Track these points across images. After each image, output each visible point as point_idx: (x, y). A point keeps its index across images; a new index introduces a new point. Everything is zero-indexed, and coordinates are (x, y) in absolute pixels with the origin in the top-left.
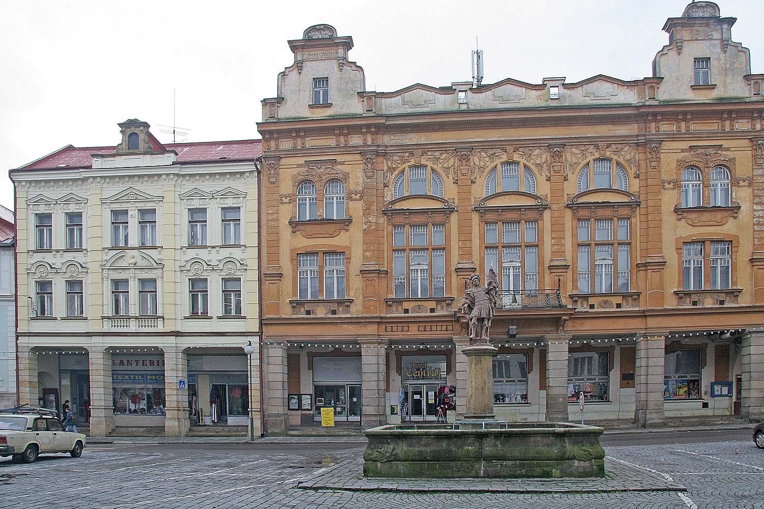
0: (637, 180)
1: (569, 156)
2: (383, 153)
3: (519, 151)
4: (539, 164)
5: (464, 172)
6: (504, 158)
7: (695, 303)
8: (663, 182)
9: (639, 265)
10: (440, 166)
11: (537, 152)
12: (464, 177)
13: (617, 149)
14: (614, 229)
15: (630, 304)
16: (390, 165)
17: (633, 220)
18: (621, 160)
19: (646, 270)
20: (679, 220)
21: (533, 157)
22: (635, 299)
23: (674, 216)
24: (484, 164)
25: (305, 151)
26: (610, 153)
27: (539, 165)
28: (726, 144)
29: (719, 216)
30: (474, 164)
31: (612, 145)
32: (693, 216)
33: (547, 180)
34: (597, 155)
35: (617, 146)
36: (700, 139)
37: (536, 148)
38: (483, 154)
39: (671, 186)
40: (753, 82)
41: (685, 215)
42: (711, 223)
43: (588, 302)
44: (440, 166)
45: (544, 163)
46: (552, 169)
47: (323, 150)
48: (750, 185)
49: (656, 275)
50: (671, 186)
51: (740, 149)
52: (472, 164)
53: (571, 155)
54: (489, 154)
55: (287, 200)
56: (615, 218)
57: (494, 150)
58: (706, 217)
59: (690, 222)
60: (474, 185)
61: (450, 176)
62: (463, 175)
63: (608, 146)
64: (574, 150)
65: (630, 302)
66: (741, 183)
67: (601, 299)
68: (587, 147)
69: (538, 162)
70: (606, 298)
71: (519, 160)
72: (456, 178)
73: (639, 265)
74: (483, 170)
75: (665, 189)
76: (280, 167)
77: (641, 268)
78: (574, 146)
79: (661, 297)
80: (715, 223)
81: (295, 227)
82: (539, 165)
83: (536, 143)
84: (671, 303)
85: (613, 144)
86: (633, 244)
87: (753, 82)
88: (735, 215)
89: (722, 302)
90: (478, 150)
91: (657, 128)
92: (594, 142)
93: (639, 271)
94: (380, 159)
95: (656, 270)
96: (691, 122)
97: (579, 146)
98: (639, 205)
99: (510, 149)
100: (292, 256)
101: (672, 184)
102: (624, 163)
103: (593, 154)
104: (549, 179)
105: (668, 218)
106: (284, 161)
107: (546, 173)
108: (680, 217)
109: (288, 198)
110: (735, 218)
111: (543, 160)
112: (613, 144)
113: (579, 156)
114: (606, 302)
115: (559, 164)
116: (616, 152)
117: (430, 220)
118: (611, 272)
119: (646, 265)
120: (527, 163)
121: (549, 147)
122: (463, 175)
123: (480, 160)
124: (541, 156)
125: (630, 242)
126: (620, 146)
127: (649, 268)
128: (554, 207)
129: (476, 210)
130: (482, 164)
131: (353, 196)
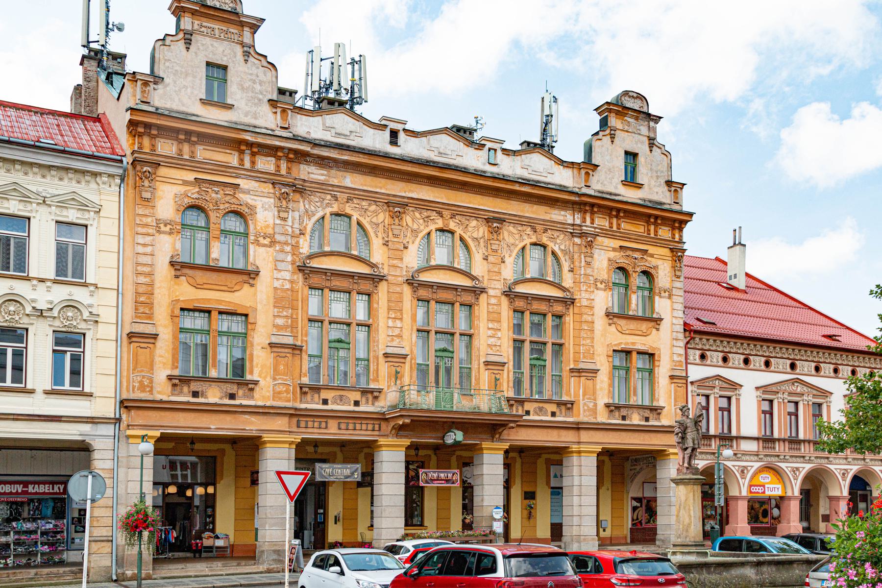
1: (506, 234)
2: (300, 189)
4: (476, 239)
5: (396, 232)
6: (440, 224)
7: (624, 418)
10: (368, 219)
11: (474, 223)
12: (396, 240)
15: (564, 414)
16: (307, 206)
20: (610, 325)
21: (470, 229)
22: (569, 409)
23: (606, 320)
25: (193, 165)
26: (546, 239)
27: (476, 239)
28: (651, 250)
29: (644, 326)
30: (407, 225)
32: (622, 322)
33: (484, 259)
34: (534, 240)
36: (630, 240)
39: (603, 286)
40: (673, 189)
41: (615, 320)
42: (637, 332)
43: (523, 407)
44: (368, 219)
46: (489, 246)
47: (224, 168)
48: (670, 297)
49: (590, 383)
50: (603, 286)
51: (662, 258)
52: (405, 224)
53: (510, 234)
55: (167, 229)
58: (633, 325)
59: (619, 329)
60: (405, 250)
61: (380, 235)
62: (396, 236)
63: (545, 231)
64: (511, 228)
65: (563, 411)
66: (663, 294)
67: (536, 405)
68: (525, 227)
69: (475, 235)
70: (541, 405)
71: (456, 229)
72: (386, 239)
74: (415, 232)
75: (597, 289)
76: (158, 179)
78: (512, 225)
79: (594, 411)
80: (640, 333)
81: (179, 270)
82: (476, 239)
83: (474, 213)
84: (603, 417)
87: (673, 189)
88: (657, 327)
89: (647, 419)
90: (411, 209)
92: (532, 224)
94: (297, 196)
96: (622, 220)
97: (517, 225)
98: (573, 303)
99: (446, 213)
100: (173, 312)
101: (604, 284)
103: (529, 237)
104: (486, 259)
105: (600, 322)
106: (162, 171)
107: (482, 250)
108: (611, 321)
109: (169, 227)
110: (658, 330)
111: (481, 235)
113: (517, 236)
114: (541, 409)
115: (497, 242)
116: (552, 239)
117: (356, 286)
119: (579, 371)
121: (488, 220)
122: (396, 236)
124: (476, 230)
126: (556, 234)
127: (583, 374)
128: (491, 292)
129: (408, 283)
130: (415, 227)
131: (261, 239)
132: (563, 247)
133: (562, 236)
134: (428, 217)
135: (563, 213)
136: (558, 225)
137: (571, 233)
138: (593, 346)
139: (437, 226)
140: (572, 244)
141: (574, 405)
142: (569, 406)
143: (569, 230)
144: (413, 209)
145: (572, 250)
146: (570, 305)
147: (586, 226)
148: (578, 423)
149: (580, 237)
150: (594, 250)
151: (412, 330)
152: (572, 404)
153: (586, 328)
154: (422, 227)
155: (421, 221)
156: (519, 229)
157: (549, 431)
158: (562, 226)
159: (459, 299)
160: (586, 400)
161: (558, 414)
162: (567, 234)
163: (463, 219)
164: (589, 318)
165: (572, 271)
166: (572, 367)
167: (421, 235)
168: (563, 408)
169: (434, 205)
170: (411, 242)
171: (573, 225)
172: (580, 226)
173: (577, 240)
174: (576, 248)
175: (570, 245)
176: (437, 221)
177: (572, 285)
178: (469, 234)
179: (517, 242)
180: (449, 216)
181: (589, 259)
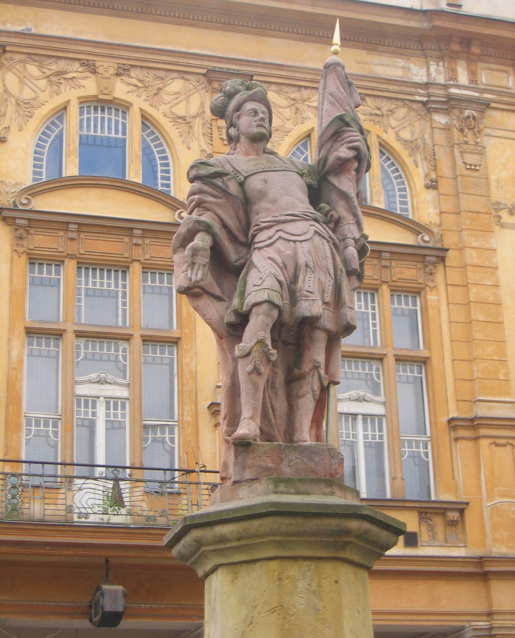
0: (431, 194)
3: (129, 76)
4: (183, 118)
8: (497, 206)
9: (456, 423)
13: (379, 109)
14: (382, 317)
15: (440, 535)
17: (431, 297)
18: (390, 138)
19: (477, 439)
21: (167, 98)
22: (453, 523)
24: (33, 95)
31: (368, 99)
35: (379, 103)
37: (176, 75)
38: (33, 69)
45: (195, 117)
54: (48, 73)
56: (385, 287)
57: (62, 65)
68: (306, 93)
69: (180, 110)
73: (456, 423)
75: (503, 226)
77: (462, 433)
85: (369, 95)
86: (435, 362)
90: (18, 57)
91: (473, 75)
93: (456, 439)
95: (504, 441)
97: (286, 89)
98: (443, 259)
102: (397, 146)
111: (194, 108)
112: (369, 95)
118: (381, 437)
120: (151, 111)
123: (22, 82)
125: (427, 355)
126: (386, 106)
127: (483, 432)
130: (27, 94)
132: (406, 135)
133: (402, 112)
134: (59, 74)
135: (401, 62)
136: (391, 87)
137: (424, 104)
138: (504, 362)
139: (82, 93)
140: (428, 130)
141: (467, 513)
142: (454, 515)
143: (418, 98)
144: (22, 57)
145: (428, 141)
146: (434, 264)
147: (458, 87)
148: (481, 560)
149: (447, 112)
150: (484, 140)
151: (11, 329)
152: (462, 511)
153: (481, 318)
154: (44, 96)
155: (43, 83)
156: (293, 96)
157: (405, 584)
158: (396, 88)
159: (138, 253)
160: (498, 500)
161: (424, 536)
162: (415, 106)
163: (150, 77)
164: (488, 295)
165: (435, 188)
166: (454, 414)
167: (41, 113)
168: (438, 522)
169: (73, 47)
170: (14, 128)
171: (426, 85)
172: (446, 87)
173: (440, 119)
174: (440, 137)
175: (423, 132)
176: (82, 82)
177: (436, 219)
178: (163, 108)
179: (289, 125)
180: (112, 71)
181: (471, 159)
